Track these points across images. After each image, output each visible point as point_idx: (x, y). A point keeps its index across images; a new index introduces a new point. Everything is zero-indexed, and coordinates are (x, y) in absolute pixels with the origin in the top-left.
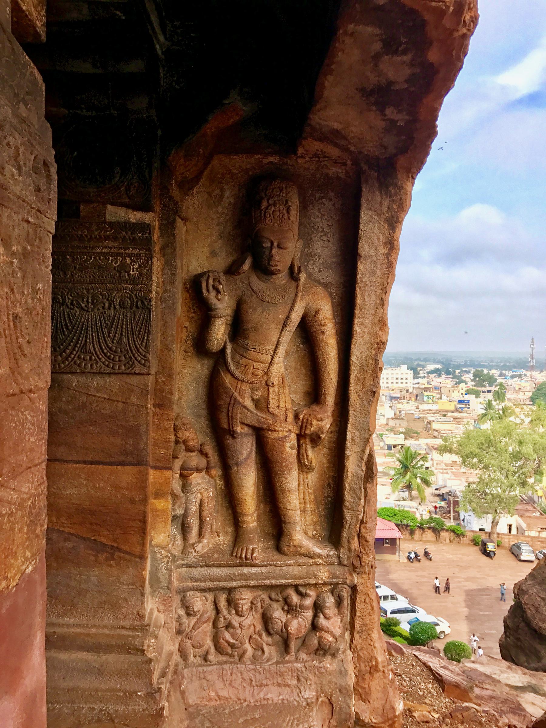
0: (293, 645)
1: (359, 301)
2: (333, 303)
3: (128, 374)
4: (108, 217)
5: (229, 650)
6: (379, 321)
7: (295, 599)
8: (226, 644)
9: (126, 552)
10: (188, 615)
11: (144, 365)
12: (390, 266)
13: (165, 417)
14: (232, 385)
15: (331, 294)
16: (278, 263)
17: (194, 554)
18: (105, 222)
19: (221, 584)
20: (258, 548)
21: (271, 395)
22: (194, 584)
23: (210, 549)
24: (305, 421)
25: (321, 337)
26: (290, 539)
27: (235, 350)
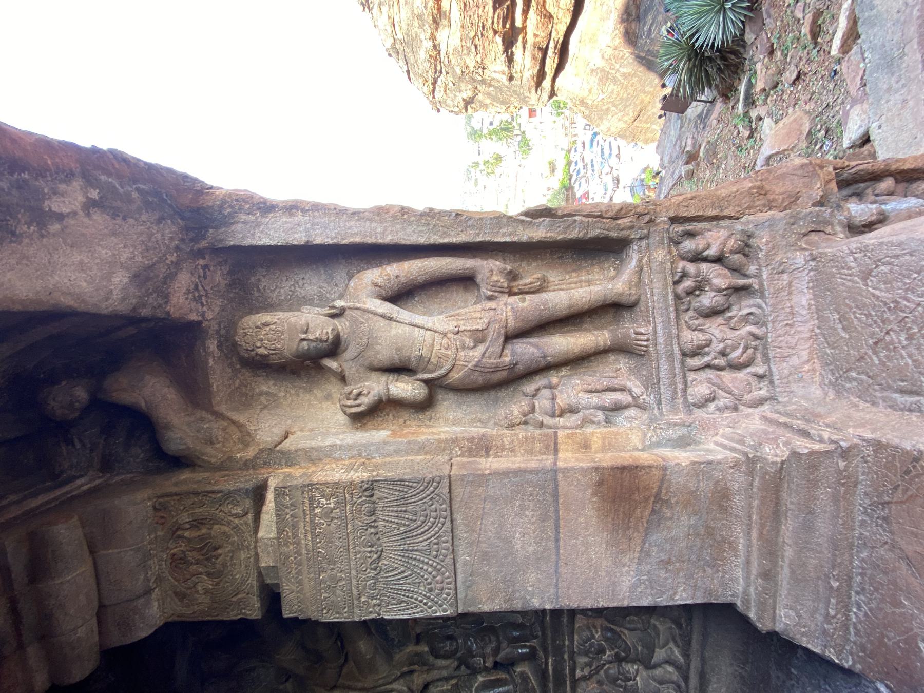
0: (742, 282)
1: (357, 240)
2: (368, 269)
3: (451, 499)
4: (272, 536)
5: (750, 351)
6: (378, 215)
7: (688, 283)
8: (745, 355)
9: (660, 488)
10: (714, 399)
11: (439, 483)
12: (316, 208)
13: (499, 444)
14: (460, 371)
15: (359, 272)
16: (325, 331)
17: (645, 396)
18: (278, 538)
19: (677, 365)
20: (631, 328)
21: (468, 328)
22: (679, 395)
23: (637, 378)
24: (493, 289)
25: (403, 279)
26: (621, 294)
27: (424, 369)
